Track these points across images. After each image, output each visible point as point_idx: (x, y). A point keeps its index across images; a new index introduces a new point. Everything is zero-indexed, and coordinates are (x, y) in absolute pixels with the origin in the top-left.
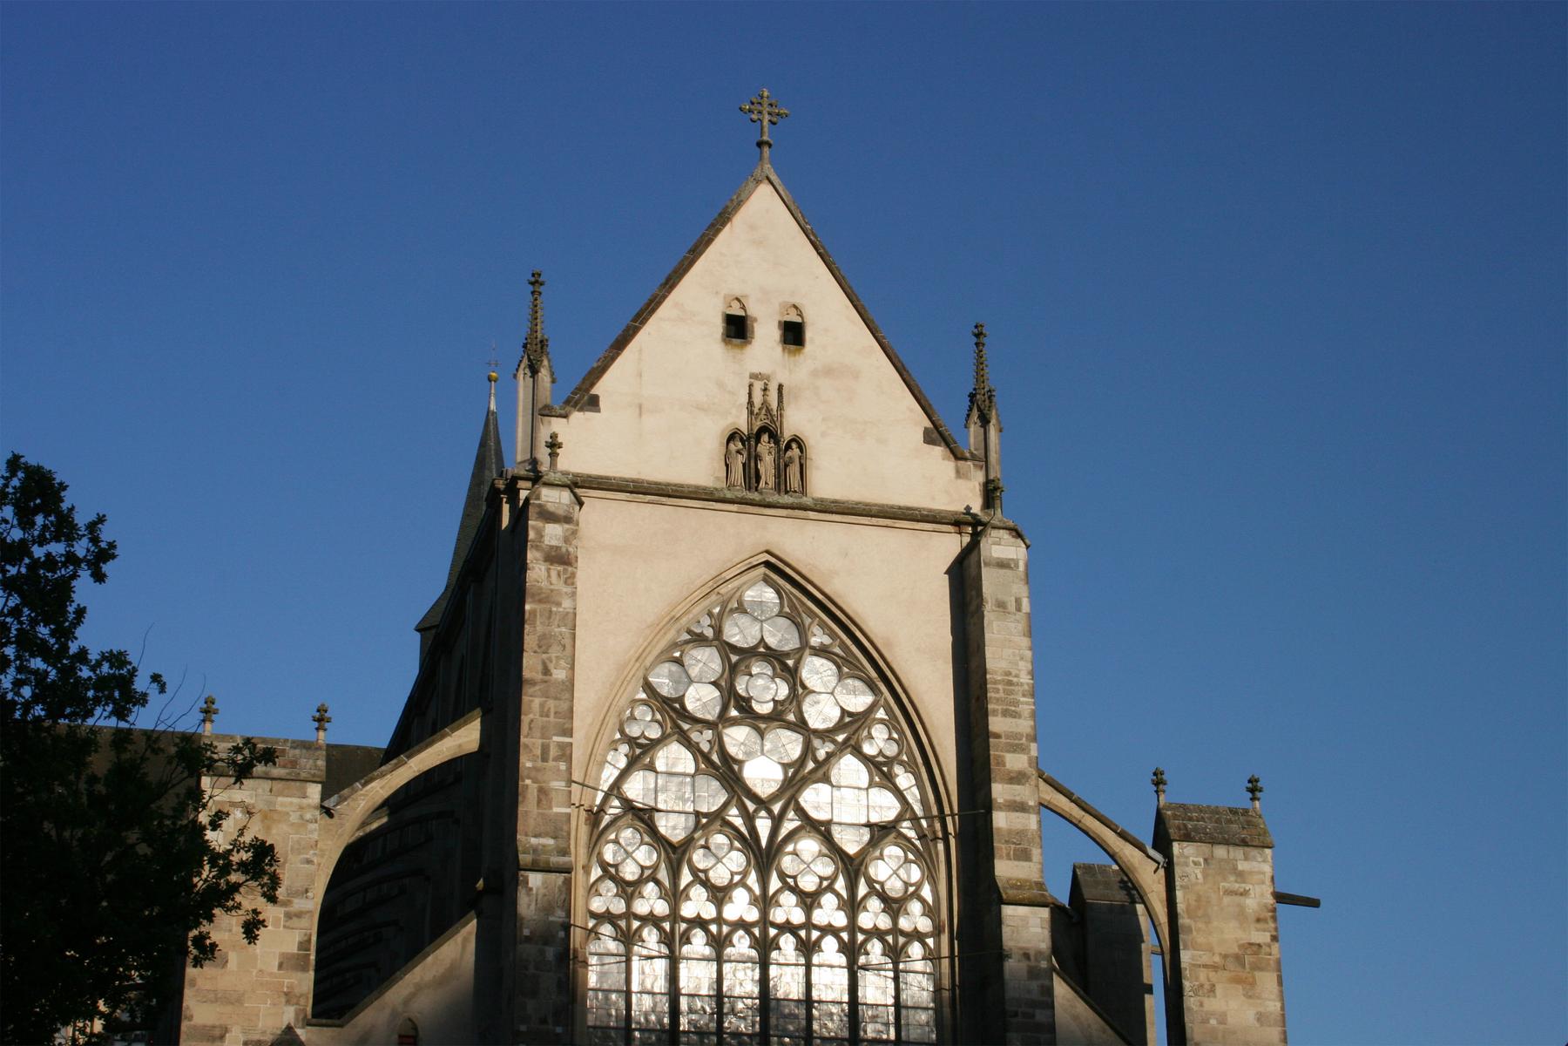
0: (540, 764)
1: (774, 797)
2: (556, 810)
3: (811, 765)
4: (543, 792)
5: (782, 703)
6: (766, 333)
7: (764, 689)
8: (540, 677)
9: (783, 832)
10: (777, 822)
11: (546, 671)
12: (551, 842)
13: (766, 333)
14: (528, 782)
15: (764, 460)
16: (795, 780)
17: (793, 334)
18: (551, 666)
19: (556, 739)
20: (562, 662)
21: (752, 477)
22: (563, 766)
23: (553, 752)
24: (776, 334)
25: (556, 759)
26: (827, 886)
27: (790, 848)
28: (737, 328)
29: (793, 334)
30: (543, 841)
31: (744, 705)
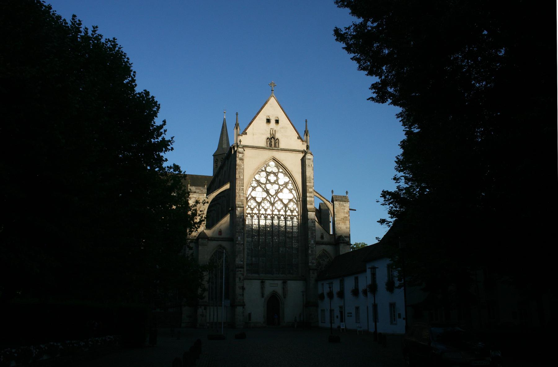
6: (273, 121)
7: (272, 178)
10: (275, 199)
13: (273, 121)
15: (273, 142)
17: (277, 122)
21: (271, 145)
24: (274, 122)
28: (268, 121)
29: (277, 122)
31: (269, 181)
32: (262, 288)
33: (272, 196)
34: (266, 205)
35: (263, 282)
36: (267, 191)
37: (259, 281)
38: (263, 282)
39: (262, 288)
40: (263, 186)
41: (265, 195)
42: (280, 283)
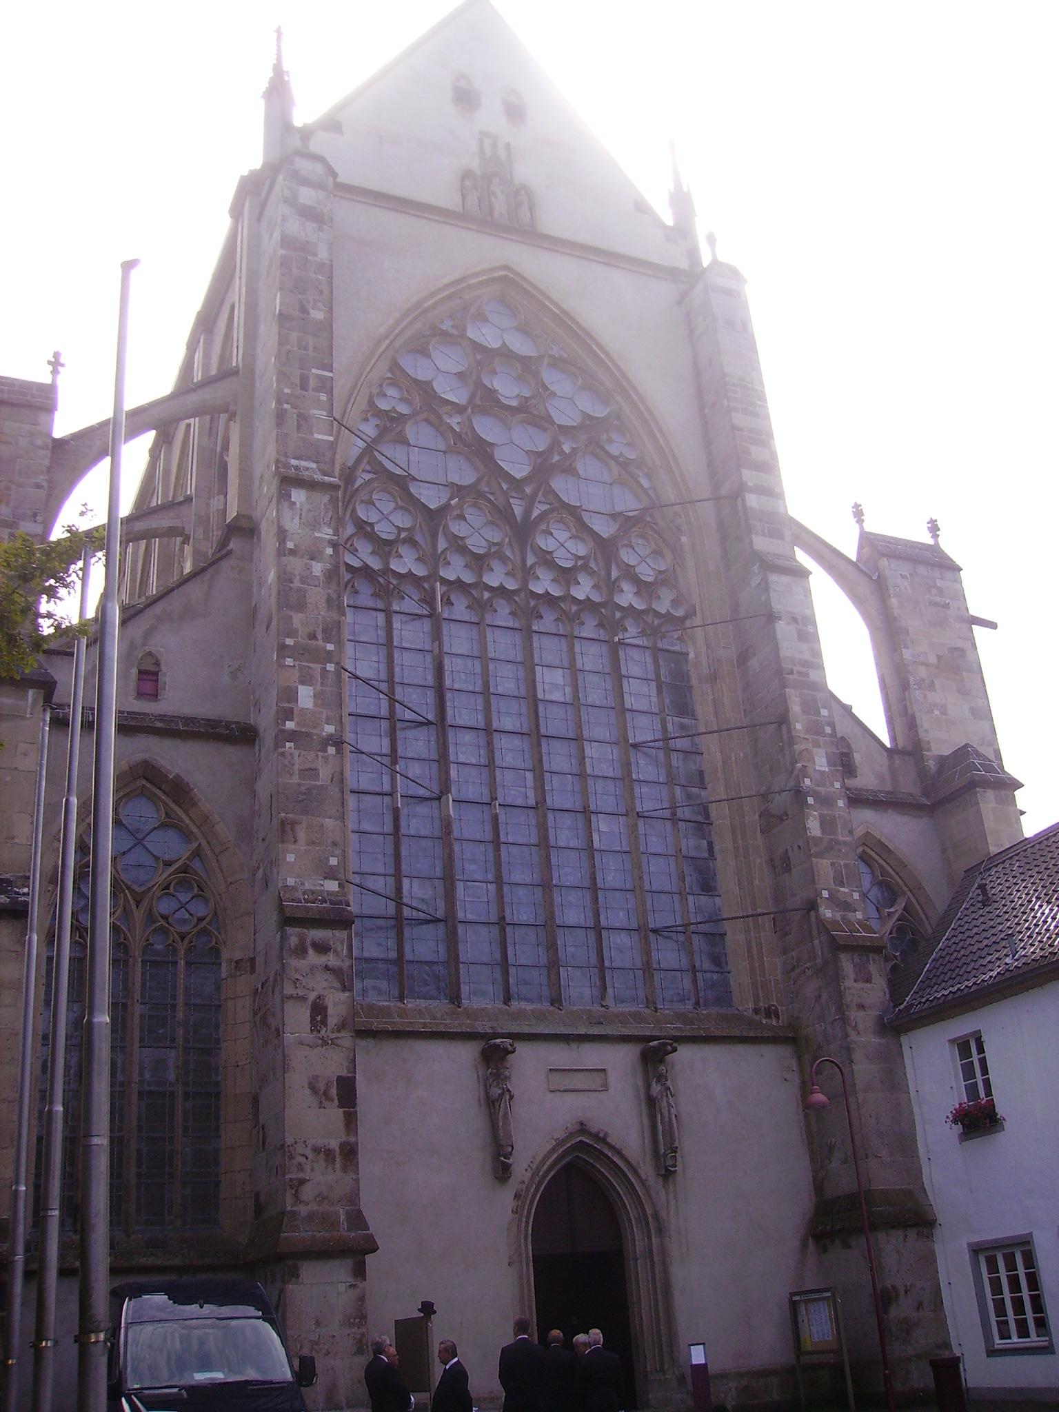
0: (299, 391)
1: (525, 480)
2: (316, 436)
3: (556, 458)
4: (303, 419)
5: (527, 399)
7: (507, 389)
9: (536, 513)
10: (530, 503)
11: (304, 310)
12: (314, 466)
14: (286, 406)
18: (309, 307)
19: (314, 371)
20: (320, 304)
22: (323, 397)
23: (312, 383)
25: (317, 390)
26: (582, 565)
27: (543, 527)
30: (304, 463)
31: (491, 395)
32: (495, 1102)
34: (477, 530)
35: (493, 1056)
36: (481, 451)
37: (467, 1053)
38: (493, 1056)
39: (495, 1102)
40: (454, 421)
41: (462, 473)
42: (619, 1061)
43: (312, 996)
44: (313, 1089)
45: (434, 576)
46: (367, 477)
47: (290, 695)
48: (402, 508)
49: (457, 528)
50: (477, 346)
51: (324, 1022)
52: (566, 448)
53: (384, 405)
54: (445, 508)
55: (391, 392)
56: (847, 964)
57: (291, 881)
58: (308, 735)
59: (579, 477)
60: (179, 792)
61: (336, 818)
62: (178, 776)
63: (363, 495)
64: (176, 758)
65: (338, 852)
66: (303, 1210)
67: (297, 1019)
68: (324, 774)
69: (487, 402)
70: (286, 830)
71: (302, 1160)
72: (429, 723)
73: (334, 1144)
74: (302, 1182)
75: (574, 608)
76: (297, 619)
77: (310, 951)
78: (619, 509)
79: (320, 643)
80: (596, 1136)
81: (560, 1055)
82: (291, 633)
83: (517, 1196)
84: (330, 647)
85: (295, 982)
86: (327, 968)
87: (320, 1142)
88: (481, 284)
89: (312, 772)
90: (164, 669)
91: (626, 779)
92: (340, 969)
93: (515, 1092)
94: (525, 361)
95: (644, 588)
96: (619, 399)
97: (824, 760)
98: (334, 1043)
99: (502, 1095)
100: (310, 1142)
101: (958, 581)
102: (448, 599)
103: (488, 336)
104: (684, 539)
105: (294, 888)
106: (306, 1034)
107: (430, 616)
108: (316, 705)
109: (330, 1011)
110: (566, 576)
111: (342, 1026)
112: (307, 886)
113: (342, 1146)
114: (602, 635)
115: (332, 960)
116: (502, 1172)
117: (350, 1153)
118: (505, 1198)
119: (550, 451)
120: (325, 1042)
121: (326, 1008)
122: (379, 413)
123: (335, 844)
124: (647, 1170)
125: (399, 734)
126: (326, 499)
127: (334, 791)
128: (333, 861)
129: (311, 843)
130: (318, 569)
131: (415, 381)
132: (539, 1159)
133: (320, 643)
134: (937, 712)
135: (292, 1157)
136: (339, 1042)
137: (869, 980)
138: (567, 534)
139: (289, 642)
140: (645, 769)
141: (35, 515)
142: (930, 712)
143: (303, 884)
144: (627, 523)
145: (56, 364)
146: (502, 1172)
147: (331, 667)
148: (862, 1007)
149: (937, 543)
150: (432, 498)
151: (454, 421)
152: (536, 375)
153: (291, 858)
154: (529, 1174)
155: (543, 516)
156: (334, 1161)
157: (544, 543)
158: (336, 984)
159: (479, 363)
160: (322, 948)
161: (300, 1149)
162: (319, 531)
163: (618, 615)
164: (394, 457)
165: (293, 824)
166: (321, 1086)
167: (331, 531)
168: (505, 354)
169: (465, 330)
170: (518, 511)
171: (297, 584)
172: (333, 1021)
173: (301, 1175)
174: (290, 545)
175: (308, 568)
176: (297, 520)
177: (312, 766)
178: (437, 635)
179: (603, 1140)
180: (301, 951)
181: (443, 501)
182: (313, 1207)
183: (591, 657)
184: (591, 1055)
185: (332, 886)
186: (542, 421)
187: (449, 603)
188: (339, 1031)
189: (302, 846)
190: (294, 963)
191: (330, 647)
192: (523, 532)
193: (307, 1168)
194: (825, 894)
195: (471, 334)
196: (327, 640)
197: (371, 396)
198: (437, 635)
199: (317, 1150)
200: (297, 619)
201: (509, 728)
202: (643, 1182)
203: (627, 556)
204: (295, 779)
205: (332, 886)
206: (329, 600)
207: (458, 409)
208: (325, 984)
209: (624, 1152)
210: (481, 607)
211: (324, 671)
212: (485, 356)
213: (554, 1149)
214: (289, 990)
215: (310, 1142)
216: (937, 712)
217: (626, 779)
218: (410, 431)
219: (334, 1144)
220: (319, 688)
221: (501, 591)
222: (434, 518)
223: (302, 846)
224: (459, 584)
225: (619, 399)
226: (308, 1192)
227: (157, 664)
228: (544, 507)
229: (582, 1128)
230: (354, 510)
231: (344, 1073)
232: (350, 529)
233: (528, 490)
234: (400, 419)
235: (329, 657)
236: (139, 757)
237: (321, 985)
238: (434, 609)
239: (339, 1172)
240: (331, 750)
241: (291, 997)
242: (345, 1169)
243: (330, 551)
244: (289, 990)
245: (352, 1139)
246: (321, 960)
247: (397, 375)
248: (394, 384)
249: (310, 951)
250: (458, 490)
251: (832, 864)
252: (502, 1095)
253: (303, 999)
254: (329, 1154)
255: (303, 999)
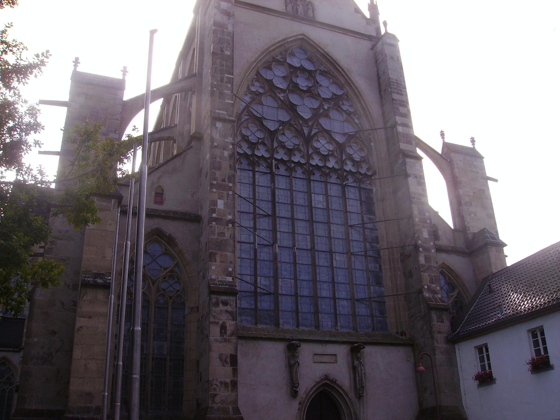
1: (309, 119)
3: (322, 111)
5: (310, 87)
7: (303, 83)
8: (219, 52)
9: (313, 133)
11: (222, 51)
12: (225, 113)
16: (317, 114)
18: (224, 50)
22: (229, 86)
23: (225, 80)
25: (227, 83)
26: (331, 154)
27: (316, 138)
31: (296, 85)
32: (292, 366)
33: (306, 121)
34: (289, 139)
35: (292, 348)
36: (292, 108)
37: (280, 347)
38: (292, 348)
39: (292, 366)
40: (281, 96)
41: (284, 116)
42: (342, 351)
43: (221, 322)
44: (220, 358)
45: (272, 157)
46: (246, 117)
47: (215, 203)
48: (260, 130)
49: (281, 138)
50: (291, 66)
51: (225, 333)
52: (326, 107)
53: (253, 89)
54: (277, 131)
55: (256, 84)
56: (434, 316)
57: (213, 277)
58: (221, 219)
59: (330, 118)
60: (170, 240)
61: (232, 252)
62: (170, 235)
63: (245, 125)
64: (170, 228)
65: (232, 265)
66: (216, 406)
67: (215, 331)
68: (227, 235)
69: (294, 88)
70: (212, 257)
71: (216, 386)
72: (269, 216)
73: (228, 381)
74: (215, 395)
75: (328, 171)
76: (218, 173)
77: (221, 304)
78: (346, 131)
79: (227, 183)
80: (331, 381)
81: (318, 348)
82: (215, 179)
83: (300, 404)
84: (231, 185)
85: (214, 317)
86: (227, 311)
87: (223, 380)
88: (293, 41)
89: (222, 234)
90: (165, 192)
91: (347, 240)
92: (232, 312)
93: (301, 362)
94: (310, 72)
95: (355, 163)
96: (347, 88)
97: (427, 234)
98: (229, 341)
99: (295, 364)
100: (219, 380)
101: (482, 162)
102: (278, 167)
103: (295, 62)
104: (372, 144)
105: (215, 280)
106: (219, 338)
107: (270, 173)
108: (224, 207)
109: (228, 328)
110: (325, 158)
111: (232, 334)
112: (220, 279)
113: (231, 382)
114: (339, 181)
115: (229, 308)
116: (294, 393)
117: (234, 384)
118: (295, 404)
119: (319, 108)
120: (225, 341)
121: (226, 327)
122: (251, 92)
123: (231, 263)
124: (352, 395)
125: (257, 220)
126: (230, 126)
127: (231, 242)
128: (230, 269)
129: (222, 262)
130: (226, 154)
131: (266, 80)
132: (309, 389)
133: (227, 183)
134: (472, 215)
135: (211, 385)
136: (231, 341)
137: (442, 322)
138: (325, 142)
139: (215, 182)
140: (355, 235)
141: (115, 131)
142: (470, 215)
143: (218, 278)
144: (350, 137)
145: (125, 71)
146: (294, 393)
147: (231, 193)
148: (439, 332)
149: (474, 147)
150: (272, 127)
151: (281, 96)
152: (314, 78)
153: (213, 268)
154: (305, 395)
155: (315, 134)
156: (228, 387)
157: (316, 144)
158: (230, 318)
159: (291, 72)
160: (225, 303)
161: (215, 382)
162: (227, 138)
163: (345, 174)
164: (257, 110)
165: (215, 254)
166: (224, 357)
167: (232, 139)
168: (302, 69)
169: (286, 59)
170: (306, 131)
171: (218, 160)
172: (229, 332)
173: (215, 393)
174: (215, 144)
175: (223, 153)
176: (218, 135)
177: (223, 231)
178: (273, 181)
179: (335, 383)
180: (217, 304)
181: (276, 127)
182: (220, 405)
183: (334, 190)
184: (331, 349)
185: (230, 279)
186: (316, 96)
187: (278, 168)
188: (231, 336)
189: (218, 263)
190: (214, 309)
191: (231, 185)
192: (308, 140)
193: (218, 390)
194: (426, 287)
195: (288, 61)
196: (230, 182)
197: (248, 86)
198: (273, 181)
199: (221, 383)
200: (218, 173)
201: (301, 218)
202: (350, 399)
203: (349, 151)
204: (216, 237)
205: (230, 279)
206: (230, 166)
207: (283, 91)
208: (226, 318)
209: (343, 387)
210: (290, 170)
211: (228, 194)
212: (294, 70)
213: (315, 386)
214: (212, 319)
215: (219, 380)
216: (472, 215)
217: (347, 240)
218: (263, 99)
219: (228, 381)
220: (226, 200)
221: (299, 163)
222: (272, 134)
223: (218, 263)
224: (282, 161)
225: (347, 88)
226: (217, 399)
227: (163, 190)
228: (316, 131)
229: (326, 377)
230: (241, 131)
231: (233, 353)
232: (239, 138)
233: (310, 123)
234: (260, 94)
235: (230, 189)
236: (155, 227)
237: (224, 318)
238: (272, 170)
239: (230, 392)
240: (230, 225)
241: (212, 322)
242: (232, 390)
243: (231, 147)
244: (212, 319)
245: (235, 379)
246: (225, 308)
247: (258, 77)
248: (257, 80)
249: (221, 304)
250: (282, 123)
251: (429, 275)
252: (295, 364)
253: (217, 323)
254: (226, 384)
255: (217, 323)
